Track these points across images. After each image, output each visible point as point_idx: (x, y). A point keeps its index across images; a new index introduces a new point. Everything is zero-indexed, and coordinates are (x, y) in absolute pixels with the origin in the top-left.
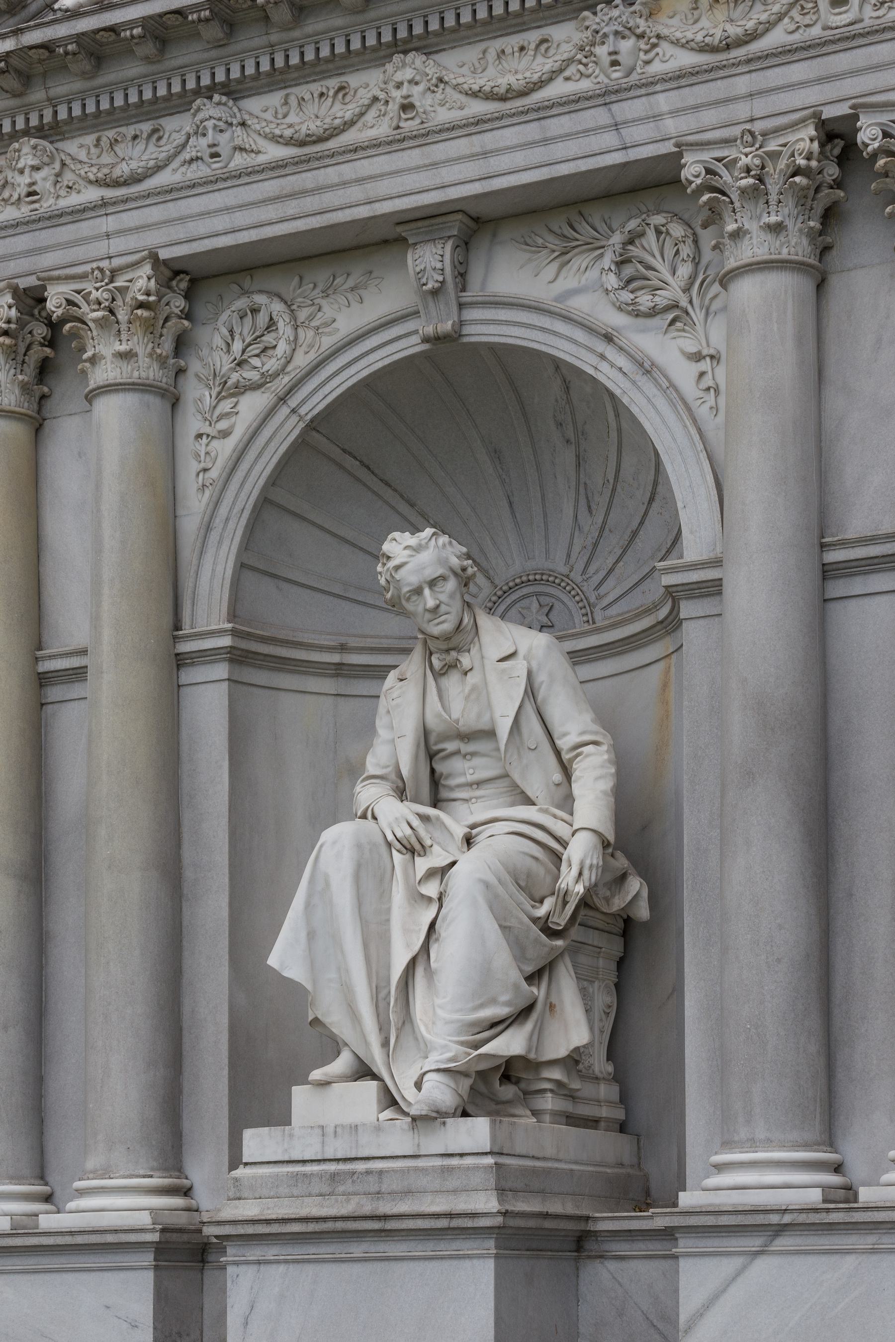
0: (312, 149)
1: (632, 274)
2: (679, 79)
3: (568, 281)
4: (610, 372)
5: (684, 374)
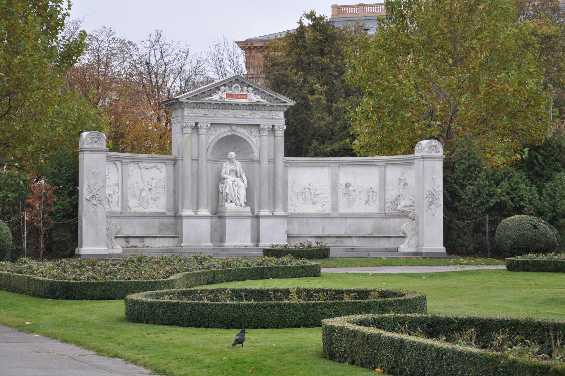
0: (225, 116)
1: (251, 132)
2: (259, 118)
3: (245, 131)
4: (248, 140)
5: (255, 142)
